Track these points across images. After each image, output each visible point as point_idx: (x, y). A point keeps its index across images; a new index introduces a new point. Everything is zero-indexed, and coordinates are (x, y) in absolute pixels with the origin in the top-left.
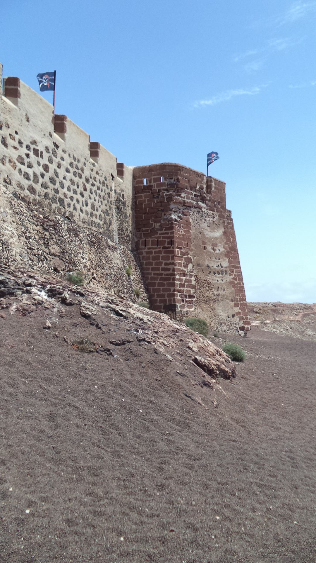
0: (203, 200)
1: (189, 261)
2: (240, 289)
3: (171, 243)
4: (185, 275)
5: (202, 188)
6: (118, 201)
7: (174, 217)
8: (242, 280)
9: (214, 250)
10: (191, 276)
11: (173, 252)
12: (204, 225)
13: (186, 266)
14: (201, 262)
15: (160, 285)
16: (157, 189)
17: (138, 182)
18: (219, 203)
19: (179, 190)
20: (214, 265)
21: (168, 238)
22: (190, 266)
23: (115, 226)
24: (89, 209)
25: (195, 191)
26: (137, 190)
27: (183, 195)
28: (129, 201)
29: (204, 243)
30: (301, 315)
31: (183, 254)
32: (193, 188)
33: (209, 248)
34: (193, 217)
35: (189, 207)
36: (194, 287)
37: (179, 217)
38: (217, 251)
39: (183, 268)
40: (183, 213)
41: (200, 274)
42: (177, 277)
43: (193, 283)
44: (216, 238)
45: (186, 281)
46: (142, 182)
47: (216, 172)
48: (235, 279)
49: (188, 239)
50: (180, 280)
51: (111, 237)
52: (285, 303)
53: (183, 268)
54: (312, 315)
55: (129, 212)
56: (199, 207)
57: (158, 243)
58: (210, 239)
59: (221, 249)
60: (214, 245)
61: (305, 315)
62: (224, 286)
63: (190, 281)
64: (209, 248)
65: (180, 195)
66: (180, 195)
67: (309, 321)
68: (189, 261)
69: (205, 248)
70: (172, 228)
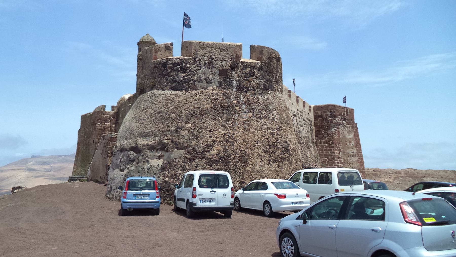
0: (345, 120)
1: (340, 151)
2: (362, 164)
3: (333, 143)
4: (338, 158)
5: (344, 114)
6: (310, 124)
7: (333, 130)
8: (362, 159)
9: (350, 144)
10: (341, 158)
11: (334, 147)
12: (346, 132)
13: (339, 154)
14: (345, 151)
15: (328, 162)
16: (325, 117)
17: (316, 113)
18: (351, 120)
19: (334, 117)
20: (350, 152)
21: (331, 140)
22: (341, 153)
23: (310, 137)
24: (304, 132)
25: (342, 116)
26: (316, 117)
27: (337, 119)
28: (313, 124)
29: (346, 142)
30: (392, 178)
31: (338, 148)
32: (340, 115)
33: (348, 144)
34: (341, 128)
35: (338, 124)
36: (342, 163)
37: (335, 130)
38: (352, 145)
39: (338, 155)
40: (337, 128)
41: (345, 157)
42: (336, 159)
43: (342, 161)
44: (351, 139)
45: (339, 160)
46: (317, 113)
47: (349, 105)
48: (359, 159)
49: (339, 140)
50: (337, 160)
51: (309, 142)
52: (381, 169)
53: (338, 155)
54: (400, 178)
55: (313, 128)
56: (343, 124)
57: (326, 143)
58: (348, 139)
59: (353, 144)
60: (350, 142)
61: (395, 178)
62: (355, 163)
63: (341, 161)
64: (348, 144)
65: (335, 119)
66: (335, 119)
67: (399, 182)
68: (340, 151)
69: (346, 144)
70: (333, 136)
